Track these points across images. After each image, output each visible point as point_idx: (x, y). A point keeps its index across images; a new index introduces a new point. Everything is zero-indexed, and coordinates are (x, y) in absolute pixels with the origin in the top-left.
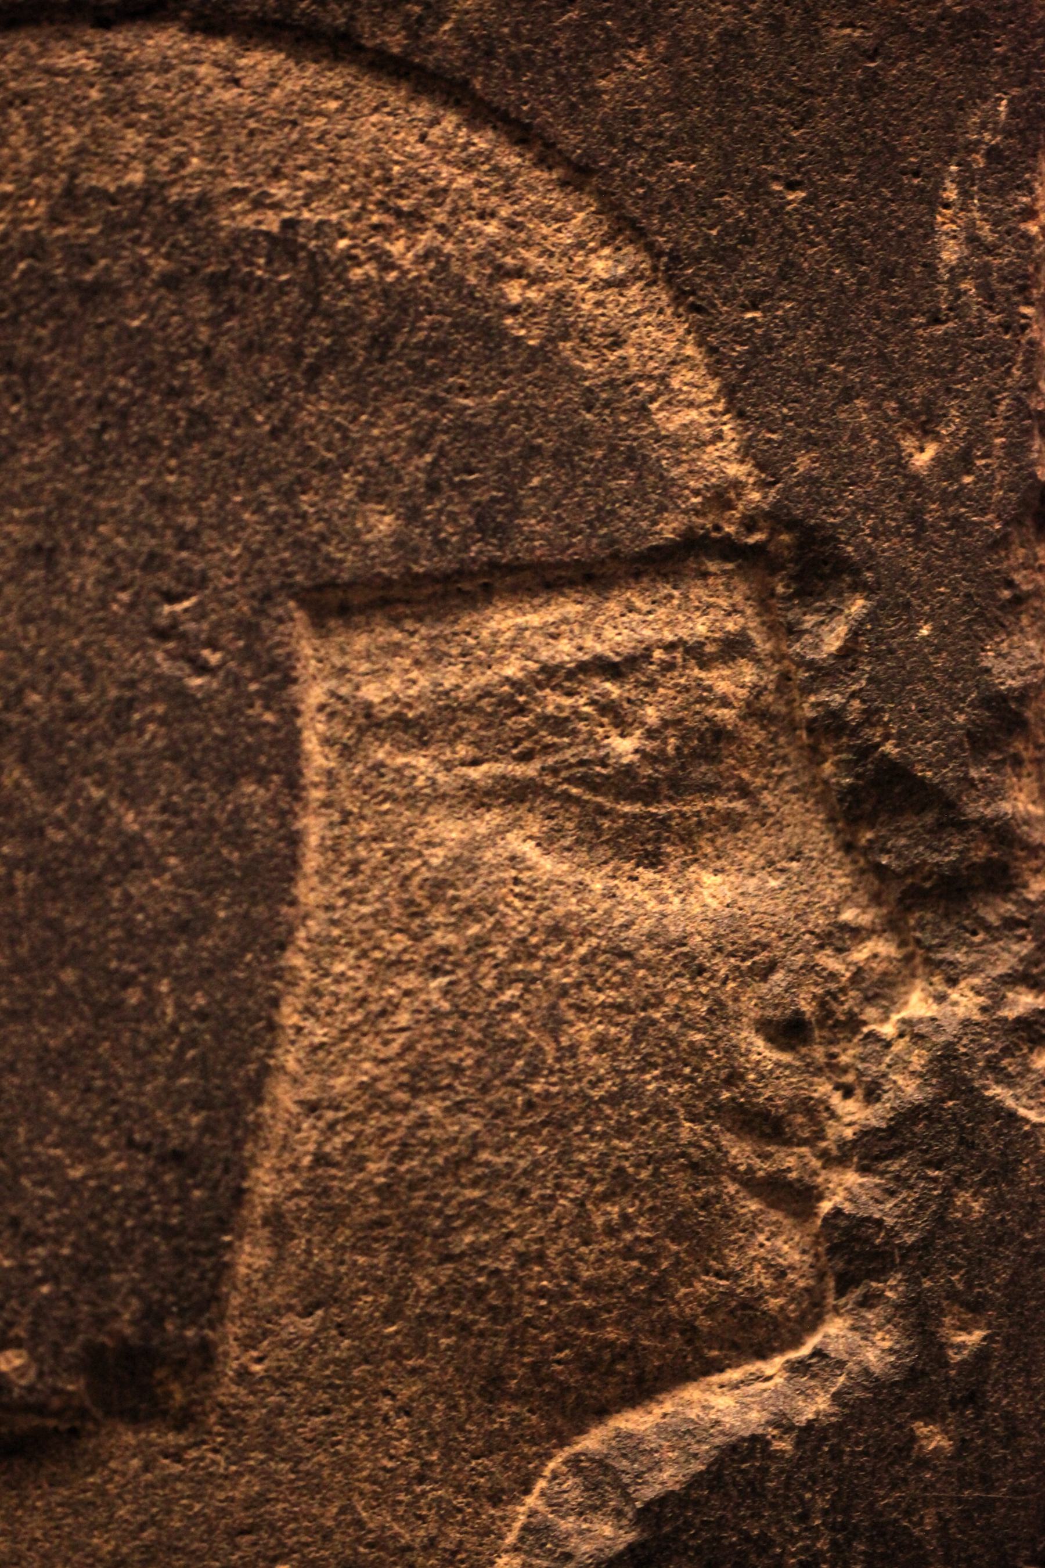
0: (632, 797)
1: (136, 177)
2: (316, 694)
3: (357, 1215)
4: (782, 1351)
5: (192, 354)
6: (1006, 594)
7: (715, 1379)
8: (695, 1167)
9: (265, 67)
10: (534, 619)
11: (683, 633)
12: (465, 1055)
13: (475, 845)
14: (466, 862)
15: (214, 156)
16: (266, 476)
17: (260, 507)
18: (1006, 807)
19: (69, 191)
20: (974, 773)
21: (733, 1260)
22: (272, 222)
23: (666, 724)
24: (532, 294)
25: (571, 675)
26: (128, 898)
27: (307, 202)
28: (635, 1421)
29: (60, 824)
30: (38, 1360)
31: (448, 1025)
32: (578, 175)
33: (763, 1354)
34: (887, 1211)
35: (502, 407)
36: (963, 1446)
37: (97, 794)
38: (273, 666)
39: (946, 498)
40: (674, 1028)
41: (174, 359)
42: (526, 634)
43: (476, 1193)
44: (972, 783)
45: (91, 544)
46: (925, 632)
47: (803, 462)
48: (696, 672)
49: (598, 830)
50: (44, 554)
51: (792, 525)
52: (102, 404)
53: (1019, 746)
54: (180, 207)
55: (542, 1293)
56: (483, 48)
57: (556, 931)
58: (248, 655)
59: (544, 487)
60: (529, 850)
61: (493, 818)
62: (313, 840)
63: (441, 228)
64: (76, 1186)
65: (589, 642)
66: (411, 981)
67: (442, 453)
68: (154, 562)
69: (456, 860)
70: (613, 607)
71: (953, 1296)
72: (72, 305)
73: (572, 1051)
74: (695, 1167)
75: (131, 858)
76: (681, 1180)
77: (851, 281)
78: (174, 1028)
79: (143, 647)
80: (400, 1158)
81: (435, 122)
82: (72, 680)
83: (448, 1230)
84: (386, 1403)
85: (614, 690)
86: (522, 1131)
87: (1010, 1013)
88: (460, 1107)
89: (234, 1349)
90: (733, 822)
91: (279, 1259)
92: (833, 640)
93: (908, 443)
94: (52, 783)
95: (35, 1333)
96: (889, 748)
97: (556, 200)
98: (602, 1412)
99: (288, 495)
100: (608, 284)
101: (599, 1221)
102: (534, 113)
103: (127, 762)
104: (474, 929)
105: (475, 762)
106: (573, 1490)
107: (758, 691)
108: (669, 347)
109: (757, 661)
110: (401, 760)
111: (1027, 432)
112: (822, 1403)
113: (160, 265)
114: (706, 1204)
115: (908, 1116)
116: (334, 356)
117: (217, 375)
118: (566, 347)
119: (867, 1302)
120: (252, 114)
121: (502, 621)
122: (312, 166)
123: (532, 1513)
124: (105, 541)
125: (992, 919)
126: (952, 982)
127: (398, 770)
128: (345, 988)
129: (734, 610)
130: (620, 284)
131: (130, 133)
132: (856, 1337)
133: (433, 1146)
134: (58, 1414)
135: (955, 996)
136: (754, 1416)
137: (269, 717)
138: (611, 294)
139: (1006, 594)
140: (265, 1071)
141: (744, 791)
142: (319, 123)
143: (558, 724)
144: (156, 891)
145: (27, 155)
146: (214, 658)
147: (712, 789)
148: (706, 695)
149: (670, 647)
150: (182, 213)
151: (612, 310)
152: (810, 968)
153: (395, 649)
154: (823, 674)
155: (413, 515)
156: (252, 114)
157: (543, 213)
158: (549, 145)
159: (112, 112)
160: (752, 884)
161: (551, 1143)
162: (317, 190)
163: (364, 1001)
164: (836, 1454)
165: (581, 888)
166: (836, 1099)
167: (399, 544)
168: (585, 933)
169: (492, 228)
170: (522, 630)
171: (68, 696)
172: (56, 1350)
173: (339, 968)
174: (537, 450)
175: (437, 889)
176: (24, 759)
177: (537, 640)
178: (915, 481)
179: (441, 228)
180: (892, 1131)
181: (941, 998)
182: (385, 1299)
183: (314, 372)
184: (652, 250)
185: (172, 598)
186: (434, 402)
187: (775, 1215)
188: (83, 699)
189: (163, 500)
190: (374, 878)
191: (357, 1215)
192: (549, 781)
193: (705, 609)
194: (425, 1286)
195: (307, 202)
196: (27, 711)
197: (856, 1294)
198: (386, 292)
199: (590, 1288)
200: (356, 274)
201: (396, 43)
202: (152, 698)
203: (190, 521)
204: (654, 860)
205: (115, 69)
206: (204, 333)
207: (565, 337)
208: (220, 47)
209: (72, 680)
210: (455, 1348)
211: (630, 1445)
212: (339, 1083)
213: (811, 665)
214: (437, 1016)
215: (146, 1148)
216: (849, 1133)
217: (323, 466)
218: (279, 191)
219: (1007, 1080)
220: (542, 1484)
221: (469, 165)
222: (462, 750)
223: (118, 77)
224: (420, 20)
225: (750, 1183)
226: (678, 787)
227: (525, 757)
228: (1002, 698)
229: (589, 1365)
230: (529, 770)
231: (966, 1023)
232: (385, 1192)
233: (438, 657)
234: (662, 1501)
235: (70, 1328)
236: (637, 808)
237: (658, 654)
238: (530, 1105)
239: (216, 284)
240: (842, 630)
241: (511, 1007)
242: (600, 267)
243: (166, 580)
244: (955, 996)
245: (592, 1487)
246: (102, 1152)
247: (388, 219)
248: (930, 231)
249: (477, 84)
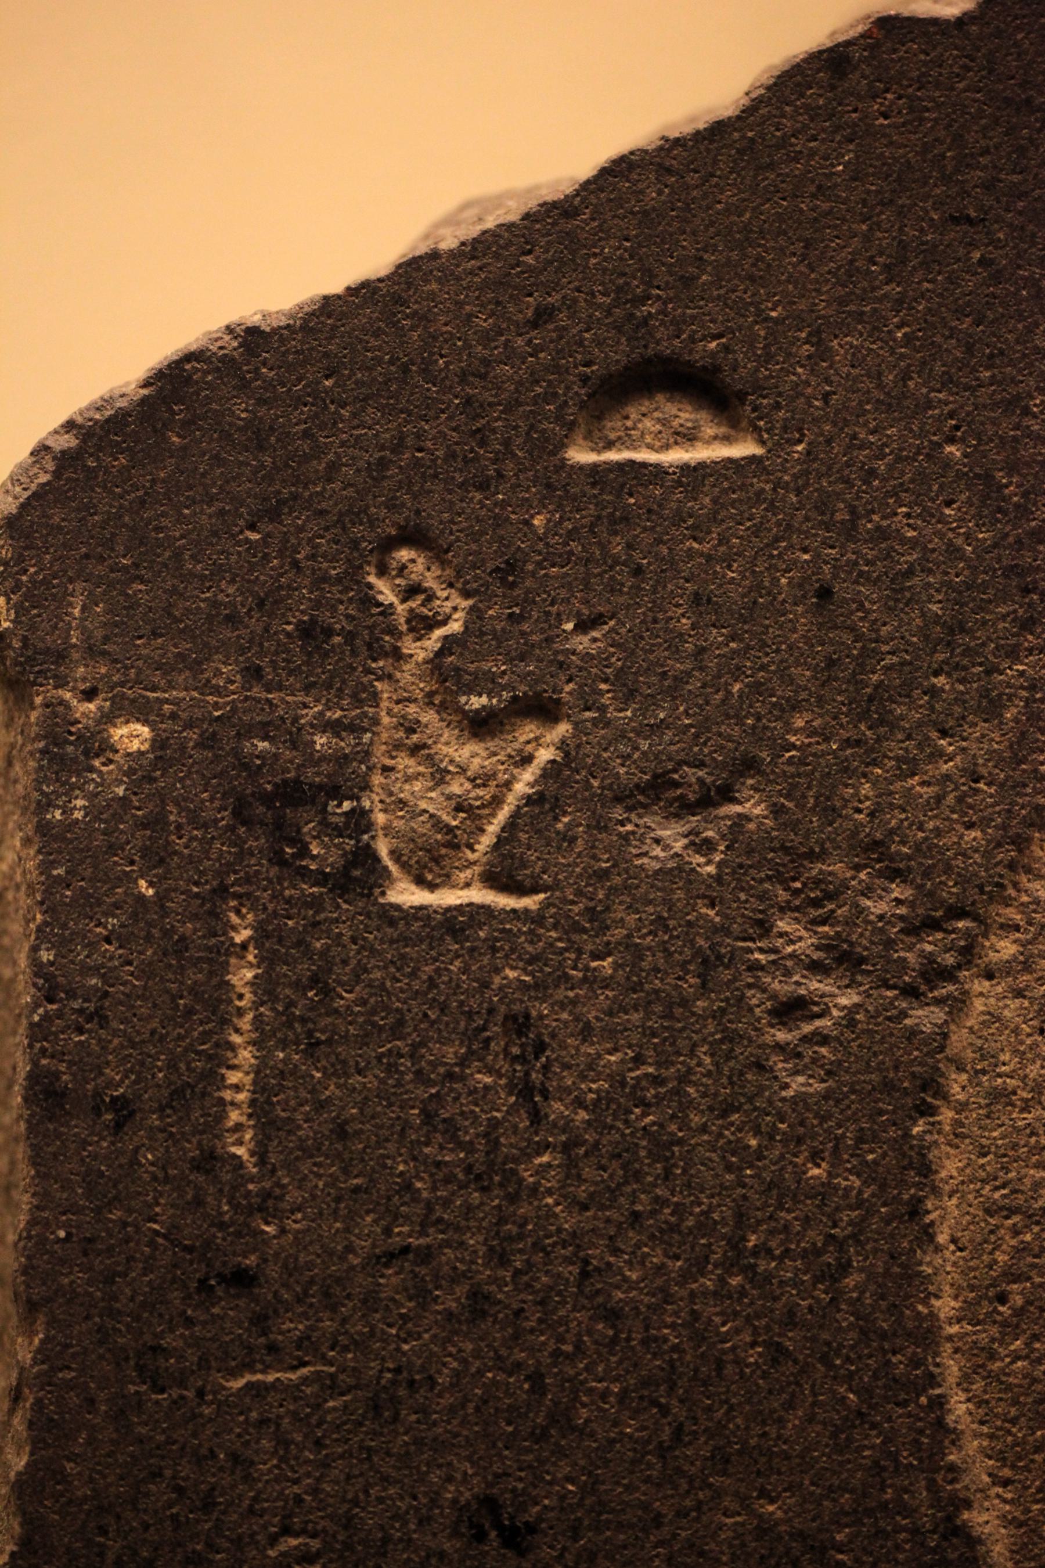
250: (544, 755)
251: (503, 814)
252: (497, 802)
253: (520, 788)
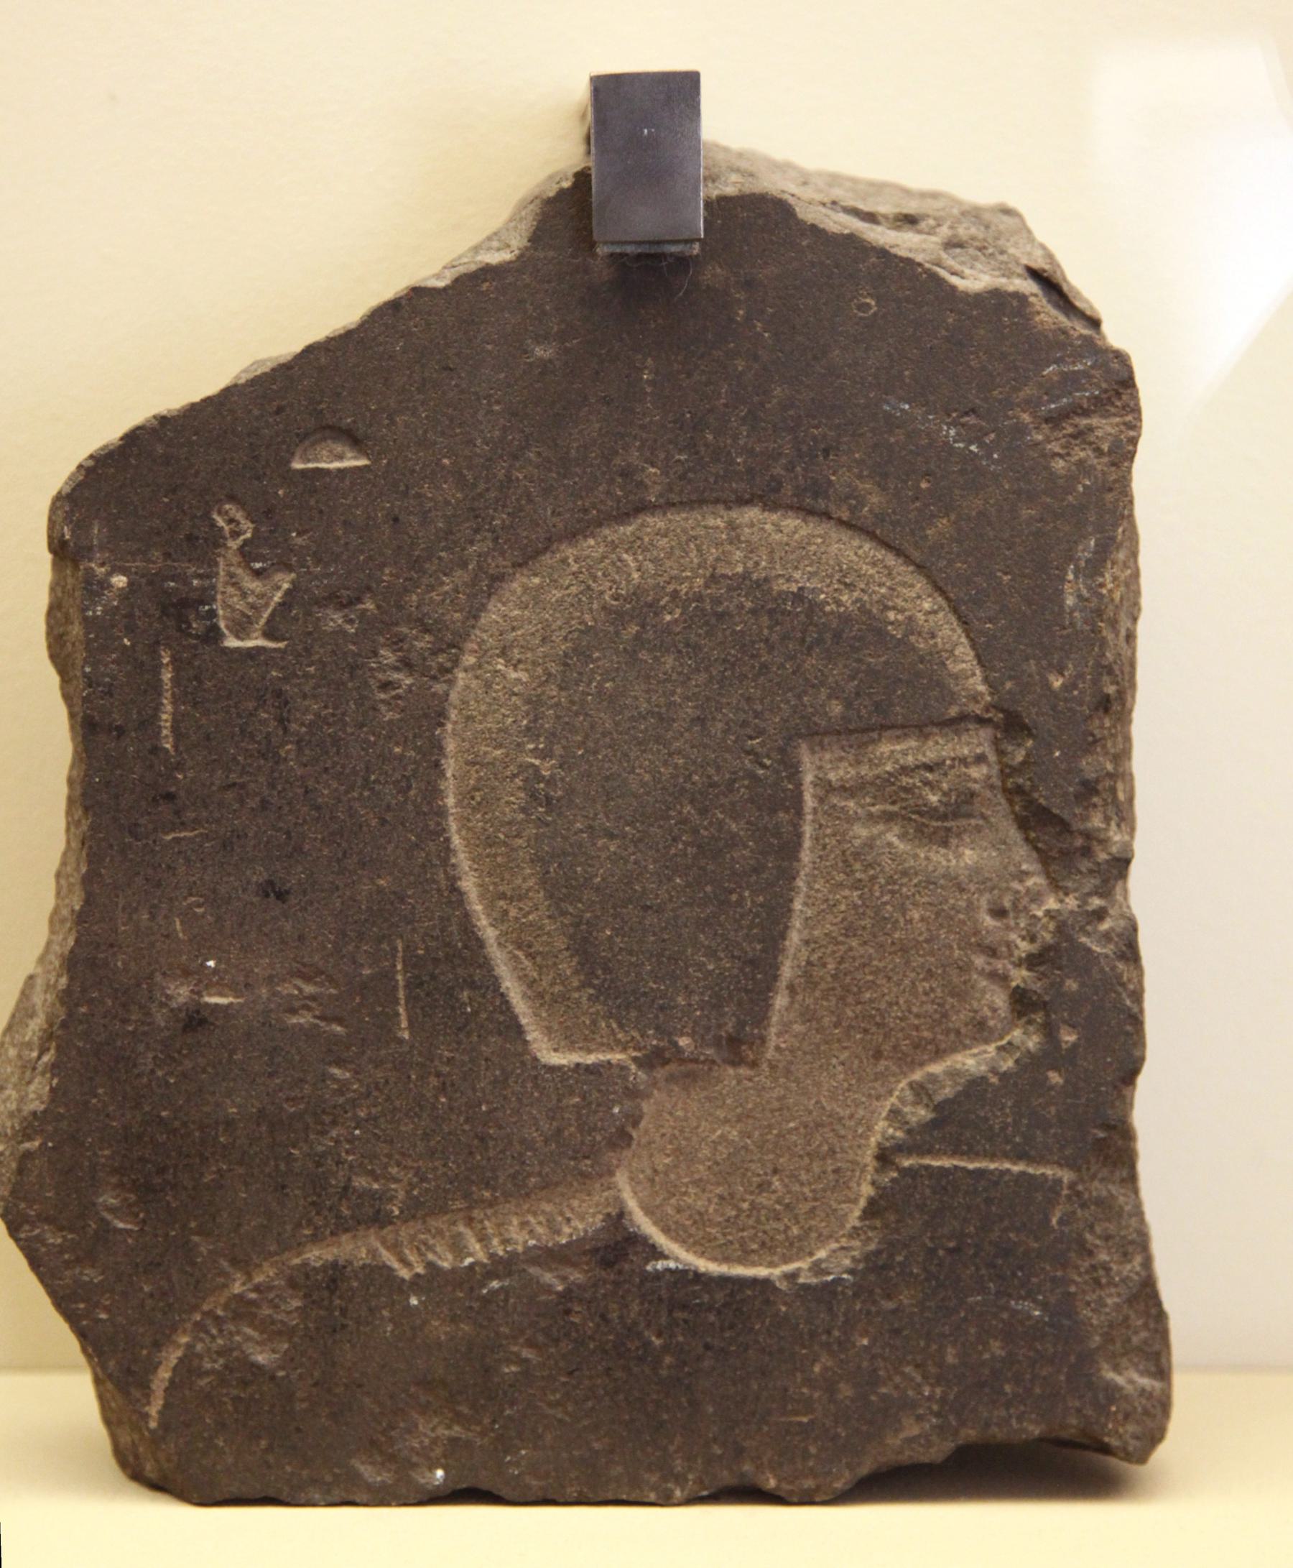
0: (937, 820)
1: (740, 569)
2: (809, 778)
3: (823, 986)
4: (996, 1041)
5: (761, 641)
6: (1090, 739)
7: (968, 1052)
8: (960, 968)
9: (792, 526)
10: (898, 748)
11: (959, 754)
12: (867, 922)
13: (873, 838)
14: (870, 844)
15: (771, 561)
16: (790, 690)
17: (788, 702)
18: (1089, 825)
19: (713, 576)
20: (1077, 811)
21: (975, 1004)
22: (794, 588)
23: (950, 790)
24: (900, 617)
25: (913, 770)
26: (732, 858)
27: (809, 579)
28: (936, 1068)
29: (706, 829)
30: (695, 1041)
31: (861, 910)
32: (920, 568)
33: (987, 1041)
34: (1037, 986)
35: (886, 663)
36: (1066, 1081)
37: (721, 816)
38: (791, 767)
39: (1066, 700)
40: (952, 913)
41: (753, 642)
42: (894, 752)
43: (870, 978)
44: (1075, 815)
45: (720, 716)
46: (1057, 754)
47: (1008, 685)
48: (964, 770)
49: (923, 833)
50: (700, 720)
51: (1002, 710)
52: (725, 661)
53: (1095, 800)
54: (757, 582)
55: (898, 1017)
56: (880, 518)
57: (905, 873)
58: (782, 762)
59: (903, 694)
60: (895, 840)
61: (881, 827)
62: (808, 835)
63: (862, 590)
64: (711, 973)
65: (920, 757)
66: (847, 892)
67: (861, 681)
68: (745, 724)
69: (865, 844)
70: (931, 743)
71: (1065, 1022)
72: (713, 621)
73: (911, 921)
74: (960, 968)
75: (734, 841)
76: (954, 972)
77: (1029, 612)
78: (751, 911)
79: (740, 758)
80: (840, 963)
81: (860, 547)
82: (711, 771)
83: (860, 992)
84: (834, 1061)
85: (929, 776)
86: (890, 954)
87: (1090, 908)
88: (865, 943)
89: (774, 1038)
90: (978, 829)
91: (792, 1003)
92: (1020, 756)
93: (1052, 678)
94: (703, 812)
95: (694, 1032)
96: (1042, 801)
97: (909, 579)
98: (922, 1064)
99: (799, 697)
100: (930, 613)
101: (920, 990)
102: (900, 544)
103: (733, 804)
104: (872, 872)
105: (873, 805)
106: (909, 1095)
107: (989, 777)
108: (955, 638)
109: (989, 766)
110: (843, 804)
111: (1101, 674)
112: (1010, 1063)
113: (749, 605)
114: (965, 982)
115: (1047, 949)
116: (820, 641)
117: (771, 648)
118: (913, 638)
119: (1030, 1022)
120: (787, 544)
121: (885, 748)
122: (810, 565)
123: (893, 1105)
124: (725, 715)
125: (1084, 870)
126: (1067, 894)
127: (842, 808)
128: (820, 895)
129: (980, 744)
130: (935, 612)
131: (738, 553)
132: (1025, 1037)
133: (854, 959)
134: (704, 1062)
135: (1067, 900)
136: (983, 1068)
137: (790, 786)
138: (931, 617)
139: (1090, 739)
140: (787, 927)
141: (983, 817)
142: (813, 548)
143: (906, 790)
144: (743, 855)
145: (696, 560)
146: (768, 762)
147: (969, 816)
148: (969, 778)
149: (953, 759)
150: (758, 584)
151: (932, 624)
152: (1008, 889)
153: (841, 759)
154: (1015, 771)
155: (848, 705)
156: (787, 544)
157: (904, 584)
158: (907, 557)
159: (731, 543)
160: (985, 854)
161: (902, 957)
162: (812, 575)
163: (827, 900)
164: (1015, 1084)
165: (916, 856)
166: (1019, 941)
167: (843, 718)
168: (916, 874)
169: (883, 590)
170: (892, 752)
171: (709, 777)
172: (703, 1037)
173: (817, 886)
174: (900, 680)
175: (857, 855)
176: (692, 802)
177: (900, 756)
178: (1054, 694)
179: (862, 590)
180: (1040, 955)
181: (1061, 901)
182: (834, 1019)
183: (810, 648)
184: (948, 599)
185: (751, 738)
186: (859, 661)
187: (993, 987)
188: (716, 778)
189: (748, 699)
190: (832, 851)
191: (823, 986)
192: (903, 812)
193: (968, 744)
194: (850, 1014)
195: (809, 579)
196: (693, 783)
197: (1024, 1019)
198: (840, 616)
199: (918, 1016)
200: (828, 608)
201: (845, 516)
202: (743, 778)
203: (759, 708)
204: (945, 844)
205: (732, 526)
206: (766, 632)
207: (912, 634)
208: (775, 517)
209: (711, 771)
210: (862, 1039)
211: (933, 1078)
212: (816, 933)
213: (1010, 767)
214: (855, 907)
215: (739, 958)
216: (1024, 955)
217: (813, 686)
218: (797, 575)
219: (1088, 934)
220: (897, 1093)
221: (874, 564)
222: (868, 800)
223: (734, 529)
224: (855, 507)
225: (982, 973)
226: (956, 815)
227: (894, 803)
228: (1088, 781)
229: (916, 1046)
230: (895, 808)
231: (1072, 912)
232: (835, 977)
233: (858, 762)
234: (947, 1101)
235: (708, 1029)
236: (939, 824)
237: (948, 762)
238: (893, 943)
239: (771, 612)
240: (1023, 753)
241: (885, 903)
242: (927, 605)
243: (749, 731)
244: (1067, 900)
245: (917, 1095)
246: (721, 959)
247: (842, 587)
248: (1062, 591)
249: (878, 532)
250: (286, 586)
251: (270, 610)
252: (267, 605)
253: (276, 599)
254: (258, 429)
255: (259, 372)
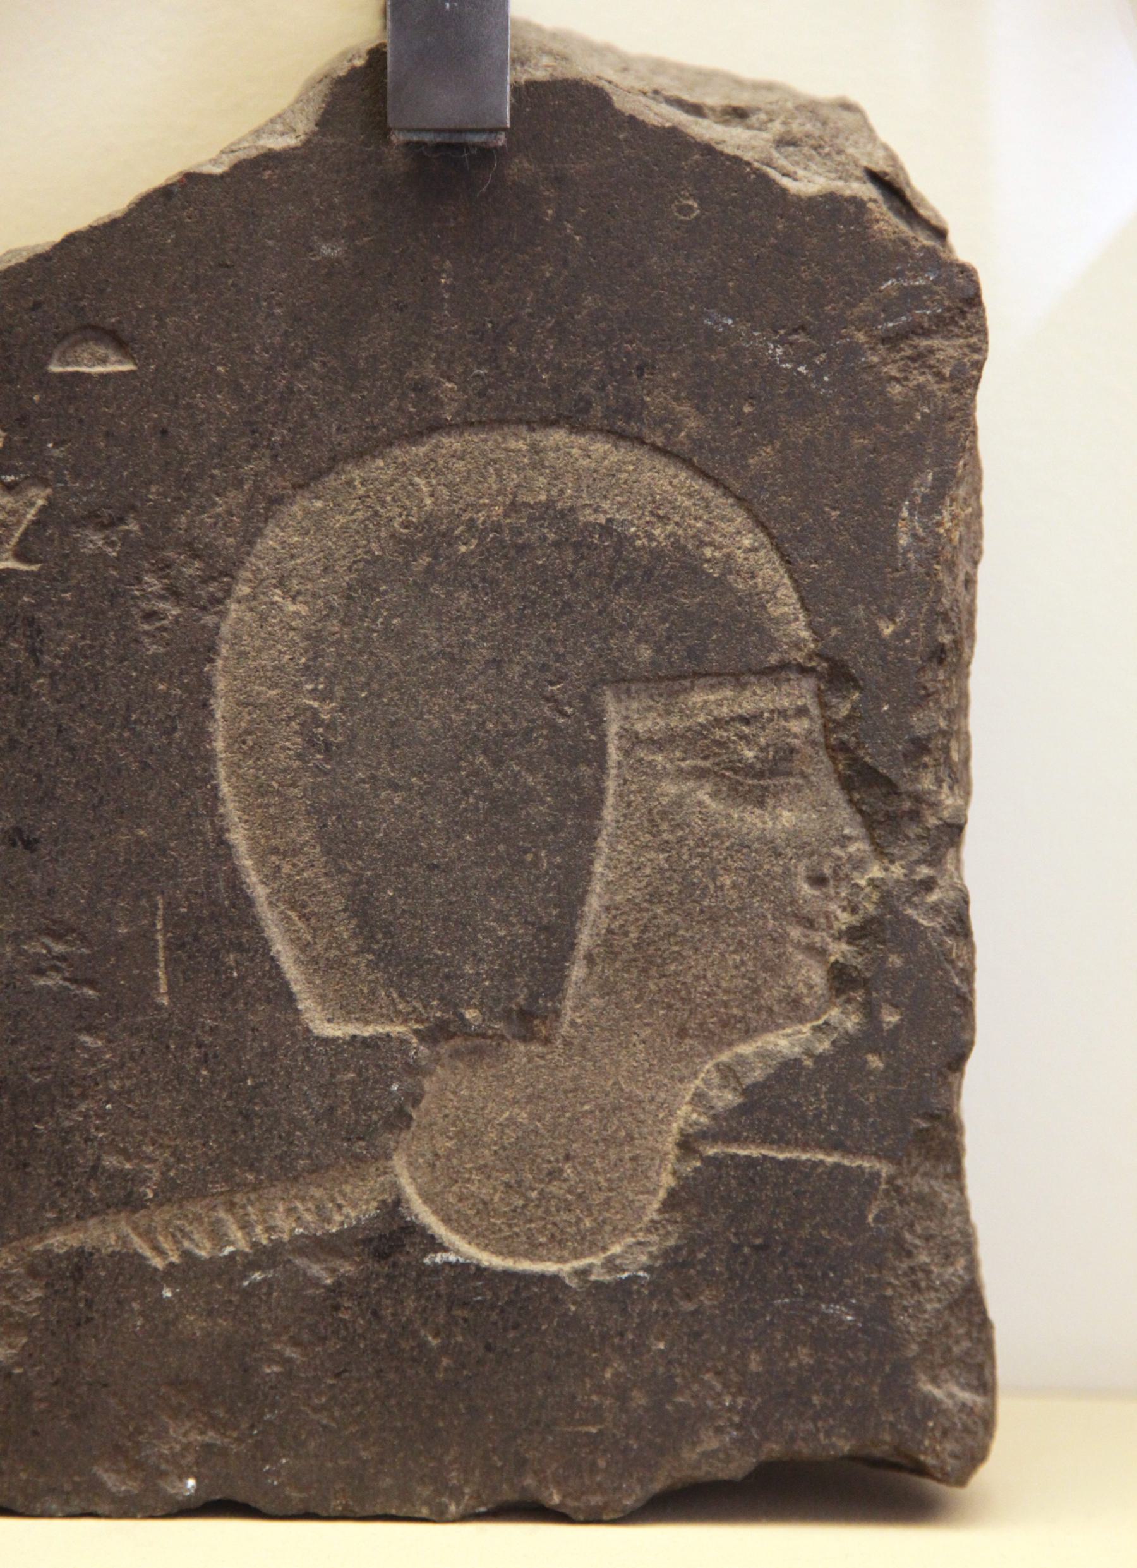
0: (754, 777)
1: (543, 497)
2: (613, 729)
3: (624, 956)
4: (811, 1020)
5: (565, 576)
6: (923, 692)
7: (781, 1032)
8: (774, 940)
9: (601, 450)
10: (712, 697)
11: (778, 706)
12: (674, 888)
13: (681, 796)
14: (679, 802)
15: (578, 489)
16: (597, 631)
17: (592, 645)
18: (919, 786)
19: (513, 503)
20: (905, 771)
21: (790, 980)
22: (602, 519)
23: (768, 745)
24: (717, 554)
25: (727, 723)
26: (528, 814)
27: (618, 511)
28: (745, 1049)
29: (500, 782)
30: (483, 1014)
31: (667, 874)
32: (740, 500)
33: (802, 1021)
34: (859, 962)
35: (701, 604)
36: (888, 1066)
37: (516, 768)
38: (595, 716)
39: (897, 649)
40: (767, 879)
41: (556, 578)
42: (707, 702)
43: (677, 948)
44: (904, 775)
45: (517, 659)
46: (886, 708)
47: (834, 631)
48: (783, 723)
49: (736, 790)
50: (497, 663)
51: (827, 659)
52: (524, 597)
53: (926, 759)
54: (562, 511)
55: (704, 992)
56: (698, 444)
57: (716, 835)
58: (584, 710)
59: (719, 639)
60: (706, 799)
61: (691, 784)
62: (611, 791)
63: (677, 524)
64: (501, 938)
65: (736, 708)
66: (652, 855)
67: (673, 623)
68: (545, 668)
69: (674, 803)
70: (748, 693)
71: (887, 1001)
72: (513, 553)
73: (721, 888)
74: (774, 940)
75: (530, 796)
76: (767, 944)
77: (858, 552)
78: (547, 872)
79: (539, 705)
80: (643, 932)
81: (676, 476)
82: (506, 718)
83: (664, 963)
84: (635, 1038)
85: (746, 729)
86: (698, 922)
87: (917, 878)
88: (671, 910)
89: (570, 1013)
90: (798, 789)
91: (590, 974)
92: (844, 710)
93: (882, 624)
94: (497, 763)
95: (482, 1003)
96: (867, 759)
97: (728, 512)
98: (730, 1044)
99: (605, 640)
100: (750, 550)
101: (731, 963)
102: (720, 474)
103: (530, 755)
104: (680, 833)
105: (684, 760)
106: (716, 1078)
107: (810, 732)
108: (777, 578)
109: (811, 719)
110: (651, 758)
111: (936, 621)
112: (826, 1045)
113: (552, 537)
114: (779, 956)
115: (869, 921)
116: (627, 579)
117: (575, 586)
118: (731, 578)
119: (849, 1001)
120: (595, 471)
121: (697, 698)
122: (621, 494)
123: (697, 1088)
124: (523, 658)
125: (912, 835)
126: (892, 862)
127: (650, 762)
128: (623, 857)
129: (802, 696)
130: (754, 550)
131: (541, 479)
132: (843, 1017)
133: (658, 927)
134: (491, 1037)
135: (893, 868)
136: (797, 1049)
137: (593, 737)
138: (752, 555)
139: (923, 692)
140: (586, 892)
141: (803, 775)
142: (624, 476)
143: (721, 744)
144: (539, 812)
145: (494, 487)
146: (569, 710)
147: (789, 774)
148: (789, 733)
149: (772, 712)
150: (562, 514)
151: (752, 562)
152: (829, 854)
153: (649, 709)
154: (840, 725)
155: (659, 650)
156: (595, 471)
157: (722, 518)
158: (726, 488)
159: (534, 468)
160: (805, 816)
161: (711, 926)
162: (622, 506)
163: (630, 863)
164: (831, 1068)
165: (728, 817)
166: (839, 912)
167: (653, 663)
168: (729, 836)
169: (699, 524)
170: (706, 702)
171: (505, 725)
172: (491, 1010)
173: (620, 847)
174: (716, 623)
175: (664, 814)
176: (484, 752)
177: (713, 707)
178: (883, 642)
179: (677, 524)
180: (862, 928)
181: (886, 869)
182: (636, 993)
183: (618, 586)
184: (770, 536)
185: (552, 683)
186: (671, 601)
187: (810, 962)
188: (512, 727)
189: (549, 641)
190: (636, 809)
191: (624, 956)
192: (716, 768)
193: (789, 695)
194: (653, 987)
195: (618, 511)
196: (487, 731)
197: (844, 997)
198: (652, 552)
199: (726, 991)
200: (638, 543)
201: (660, 441)
202: (542, 727)
203: (562, 650)
204: (761, 804)
205: (535, 449)
206: (570, 567)
207: (731, 573)
208: (582, 440)
209: (506, 718)
210: (665, 1015)
211: (741, 1060)
212: (618, 898)
213: (834, 721)
214: (662, 871)
215: (533, 924)
216: (844, 927)
217: (621, 628)
218: (606, 505)
219: (916, 907)
220: (702, 1075)
221: (690, 495)
222: (678, 754)
223: (537, 453)
224: (671, 431)
225: (798, 945)
226: (774, 773)
227: (706, 758)
228: (919, 739)
229: (724, 1024)
230: (707, 764)
231: (897, 881)
232: (637, 947)
233: (669, 713)
234: (755, 1085)
235: (497, 1001)
236: (755, 782)
237: (766, 715)
238: (702, 911)
239: (577, 546)
240: (849, 706)
241: (694, 868)
242: (747, 542)
243: (549, 676)
244: (893, 868)
245: (725, 1077)
246: (513, 925)
247: (655, 519)
248: (895, 530)
249: (695, 460)
250: (40, 502)
251: (21, 529)
252: (19, 523)
254: (11, 326)
255: (13, 262)
